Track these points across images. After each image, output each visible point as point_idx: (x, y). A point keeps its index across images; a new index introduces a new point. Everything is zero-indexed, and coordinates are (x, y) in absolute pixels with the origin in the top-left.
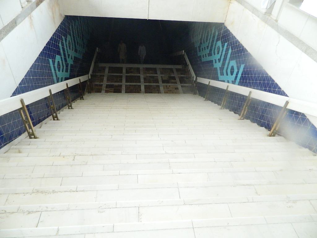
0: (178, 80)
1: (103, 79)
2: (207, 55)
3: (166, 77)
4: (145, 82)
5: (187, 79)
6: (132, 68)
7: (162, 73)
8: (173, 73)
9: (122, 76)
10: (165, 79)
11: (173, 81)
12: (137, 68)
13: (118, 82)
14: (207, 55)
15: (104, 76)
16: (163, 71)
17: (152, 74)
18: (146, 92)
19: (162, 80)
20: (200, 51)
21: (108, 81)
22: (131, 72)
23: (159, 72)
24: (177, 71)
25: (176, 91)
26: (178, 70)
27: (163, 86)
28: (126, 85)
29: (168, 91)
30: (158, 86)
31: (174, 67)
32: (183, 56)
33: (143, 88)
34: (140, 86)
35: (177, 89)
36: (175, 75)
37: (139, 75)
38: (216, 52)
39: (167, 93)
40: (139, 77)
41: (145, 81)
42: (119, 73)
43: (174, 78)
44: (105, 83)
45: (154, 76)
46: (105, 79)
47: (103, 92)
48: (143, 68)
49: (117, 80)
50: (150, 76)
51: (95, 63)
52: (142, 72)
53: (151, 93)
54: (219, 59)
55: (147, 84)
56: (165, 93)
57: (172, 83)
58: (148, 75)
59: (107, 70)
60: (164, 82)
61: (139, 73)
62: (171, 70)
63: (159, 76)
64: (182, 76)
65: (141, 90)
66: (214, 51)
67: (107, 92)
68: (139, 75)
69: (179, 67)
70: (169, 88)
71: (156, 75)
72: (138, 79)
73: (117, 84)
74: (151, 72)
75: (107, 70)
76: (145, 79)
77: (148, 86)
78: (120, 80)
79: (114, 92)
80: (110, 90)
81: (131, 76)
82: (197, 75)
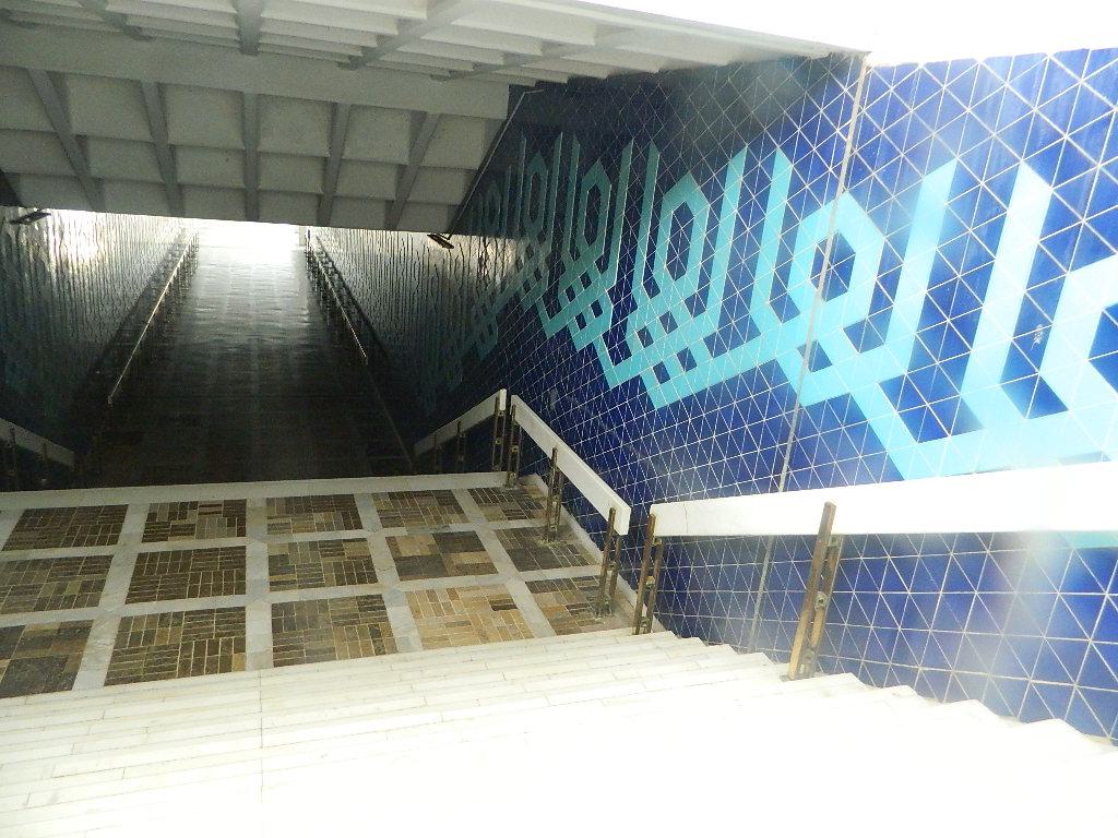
0: (496, 550)
2: (700, 352)
3: (417, 540)
4: (275, 585)
5: (553, 536)
6: (194, 505)
7: (388, 520)
8: (460, 511)
9: (109, 558)
10: (418, 552)
11: (467, 558)
12: (227, 503)
13: (70, 603)
14: (700, 352)
16: (397, 509)
20: (621, 353)
22: (188, 531)
23: (369, 515)
24: (478, 501)
25: (499, 619)
26: (483, 497)
27: (409, 594)
28: (125, 622)
29: (449, 625)
30: (374, 605)
31: (458, 483)
33: (258, 629)
34: (236, 618)
35: (504, 605)
37: (236, 542)
38: (801, 286)
39: (443, 641)
40: (237, 558)
41: (276, 578)
42: (91, 543)
43: (472, 542)
45: (339, 543)
48: (270, 502)
49: (61, 589)
50: (313, 545)
52: (256, 524)
56: (429, 642)
57: (464, 570)
58: (299, 538)
60: (408, 568)
61: (242, 533)
62: (446, 500)
63: (373, 535)
64: (516, 524)
65: (241, 647)
68: (236, 542)
69: (492, 480)
70: (449, 610)
72: (230, 570)
73: (51, 619)
74: (319, 517)
76: (278, 564)
77: (300, 605)
78: (85, 587)
81: (176, 554)
82: (640, 495)
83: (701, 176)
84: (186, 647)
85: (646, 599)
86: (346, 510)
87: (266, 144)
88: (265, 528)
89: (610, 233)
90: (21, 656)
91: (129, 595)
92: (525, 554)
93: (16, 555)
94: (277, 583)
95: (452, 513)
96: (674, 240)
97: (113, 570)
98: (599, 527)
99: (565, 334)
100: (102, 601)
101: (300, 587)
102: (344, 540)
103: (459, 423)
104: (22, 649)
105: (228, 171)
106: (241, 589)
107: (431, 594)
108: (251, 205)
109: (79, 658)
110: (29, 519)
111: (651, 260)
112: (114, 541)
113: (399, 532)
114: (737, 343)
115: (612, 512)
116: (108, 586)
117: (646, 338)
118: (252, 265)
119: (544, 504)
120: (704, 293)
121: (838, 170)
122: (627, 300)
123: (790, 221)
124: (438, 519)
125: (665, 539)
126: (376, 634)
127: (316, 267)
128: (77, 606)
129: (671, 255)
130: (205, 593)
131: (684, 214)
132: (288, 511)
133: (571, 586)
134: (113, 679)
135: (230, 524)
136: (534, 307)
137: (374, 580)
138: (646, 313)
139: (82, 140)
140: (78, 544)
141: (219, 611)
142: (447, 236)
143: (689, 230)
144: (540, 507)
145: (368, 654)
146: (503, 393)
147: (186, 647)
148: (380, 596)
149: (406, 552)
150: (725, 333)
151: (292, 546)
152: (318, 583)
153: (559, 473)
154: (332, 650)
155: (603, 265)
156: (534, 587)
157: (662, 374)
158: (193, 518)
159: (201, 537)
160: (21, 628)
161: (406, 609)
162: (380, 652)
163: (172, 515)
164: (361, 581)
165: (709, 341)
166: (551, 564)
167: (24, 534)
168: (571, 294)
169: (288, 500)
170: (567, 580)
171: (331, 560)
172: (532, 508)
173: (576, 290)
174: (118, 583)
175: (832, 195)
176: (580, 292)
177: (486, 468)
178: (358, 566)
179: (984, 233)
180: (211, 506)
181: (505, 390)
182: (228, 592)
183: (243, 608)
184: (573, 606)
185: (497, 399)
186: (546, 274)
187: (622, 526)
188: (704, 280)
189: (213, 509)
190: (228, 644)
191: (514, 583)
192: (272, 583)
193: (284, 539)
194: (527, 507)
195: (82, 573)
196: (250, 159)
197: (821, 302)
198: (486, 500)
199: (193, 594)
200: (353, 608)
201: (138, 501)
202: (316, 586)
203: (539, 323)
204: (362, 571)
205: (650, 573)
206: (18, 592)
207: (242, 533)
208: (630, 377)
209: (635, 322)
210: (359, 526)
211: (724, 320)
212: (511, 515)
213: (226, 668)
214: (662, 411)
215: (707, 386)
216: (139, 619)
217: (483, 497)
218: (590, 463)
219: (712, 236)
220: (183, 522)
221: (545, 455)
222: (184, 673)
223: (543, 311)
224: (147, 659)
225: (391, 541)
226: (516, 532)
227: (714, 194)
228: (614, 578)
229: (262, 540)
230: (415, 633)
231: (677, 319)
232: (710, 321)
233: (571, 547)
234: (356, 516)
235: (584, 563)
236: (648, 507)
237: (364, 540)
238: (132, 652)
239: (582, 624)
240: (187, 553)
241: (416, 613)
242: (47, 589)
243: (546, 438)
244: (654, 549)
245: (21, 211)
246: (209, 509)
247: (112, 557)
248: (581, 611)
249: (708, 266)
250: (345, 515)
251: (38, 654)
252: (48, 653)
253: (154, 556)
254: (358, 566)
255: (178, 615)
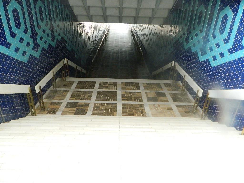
0: (169, 97)
1: (66, 95)
2: (226, 53)
3: (152, 94)
6: (108, 83)
7: (146, 89)
8: (162, 88)
11: (163, 98)
13: (86, 99)
14: (226, 53)
15: (68, 91)
16: (148, 87)
17: (134, 89)
18: (124, 114)
19: (147, 97)
21: (72, 98)
22: (106, 88)
23: (142, 87)
24: (166, 86)
25: (169, 112)
26: (167, 85)
28: (95, 104)
30: (141, 106)
31: (162, 82)
32: (173, 69)
33: (119, 108)
34: (115, 106)
35: (170, 109)
36: (165, 91)
37: (115, 90)
39: (156, 115)
43: (163, 95)
44: (67, 99)
45: (135, 93)
46: (69, 95)
47: (59, 113)
49: (84, 97)
50: (130, 92)
51: (57, 75)
52: (119, 87)
53: (132, 115)
55: (126, 102)
56: (153, 115)
57: (162, 101)
58: (127, 91)
59: (75, 85)
60: (150, 99)
61: (116, 89)
62: (159, 85)
63: (143, 92)
64: (174, 92)
65: (116, 111)
67: (64, 113)
68: (115, 90)
70: (158, 109)
71: (138, 91)
72: (114, 96)
74: (132, 87)
75: (75, 85)
76: (123, 96)
77: (127, 104)
78: (88, 97)
79: (76, 113)
80: (70, 110)
82: (205, 88)
83: (232, 6)
84: (106, 110)
85: (205, 112)
86: (137, 86)
87: (124, 6)
88: (121, 88)
89: (204, 23)
90: (77, 108)
91: (96, 99)
92: (175, 99)
93: (77, 89)
94: (123, 99)
95: (160, 88)
96: (222, 24)
97: (93, 94)
98: (194, 94)
99: (190, 48)
100: (91, 99)
101: (127, 101)
102: (137, 92)
103: (163, 68)
104: (78, 107)
105: (116, 12)
106: (116, 100)
107: (154, 105)
108: (120, 20)
109: (88, 109)
110: (79, 83)
111: (215, 30)
112: (93, 88)
113: (148, 91)
114: (237, 50)
115: (198, 91)
116: (92, 97)
117: (211, 49)
118: (120, 33)
119: (181, 88)
120: (229, 38)
122: (207, 40)
124: (157, 90)
125: (211, 98)
126: (142, 112)
128: (87, 100)
129: (221, 28)
130: (109, 100)
131: (226, 17)
132: (126, 85)
133: (186, 107)
134: (93, 114)
135: (114, 87)
136: (183, 42)
137: (142, 101)
138: (213, 43)
139: (89, 7)
140: (87, 88)
141: (112, 104)
142: (163, 25)
143: (226, 21)
144: (180, 88)
145: (140, 116)
146: (173, 62)
147: (106, 110)
148: (143, 104)
149: (149, 96)
150: (234, 48)
151: (126, 92)
152: (131, 100)
153: (185, 81)
154: (133, 114)
155: (201, 31)
156: (177, 106)
157: (215, 58)
158: (107, 85)
159: (109, 89)
160: (78, 103)
161: (149, 108)
162: (143, 116)
163: (104, 84)
164: (140, 101)
165: (229, 50)
166: (181, 101)
167: (79, 86)
168: (192, 38)
169: (126, 83)
170: (185, 106)
171: (134, 96)
172: (178, 88)
173: (194, 37)
174: (94, 96)
176: (195, 38)
177: (168, 79)
178: (139, 98)
180: (111, 83)
181: (174, 61)
182: (114, 100)
183: (116, 104)
184: (187, 111)
185: (172, 63)
186: (186, 33)
187: (200, 94)
188: (229, 34)
189: (112, 84)
190: (113, 110)
191: (173, 105)
192: (122, 99)
193: (125, 91)
194: (177, 88)
195: (88, 94)
196: (121, 9)
198: (167, 86)
199: (107, 100)
200: (138, 106)
201: (98, 81)
202: (130, 101)
203: (183, 46)
204: (139, 99)
205: (206, 106)
206: (77, 96)
207: (116, 89)
208: (206, 59)
209: (209, 45)
210: (140, 89)
211: (234, 44)
212: (173, 90)
213: (113, 115)
214: (214, 67)
215: (227, 62)
216: (98, 104)
217: (167, 85)
218: (194, 80)
219: (233, 23)
220: (106, 86)
221: (182, 77)
222: (105, 115)
223: (185, 43)
224: (99, 111)
225: (146, 93)
226: (174, 94)
227: (235, 11)
228: (197, 106)
229: (120, 91)
230: (150, 113)
231: (220, 45)
232: (230, 45)
233: (187, 98)
234: (139, 87)
235: (190, 102)
236: (207, 90)
237: (141, 92)
238: (97, 109)
239: (188, 115)
240: (106, 92)
241: (151, 109)
242: (82, 96)
243: (183, 73)
244: (208, 101)
245: (78, 23)
246: (110, 83)
247: (93, 91)
248: (188, 112)
249: (231, 30)
250: (137, 87)
251: (81, 108)
252: (82, 108)
253: (100, 92)
254: (139, 98)
255: (104, 104)
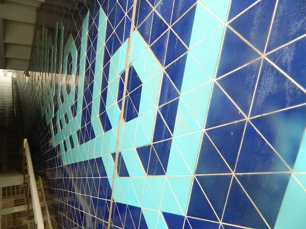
54: (143, 152)
66: (103, 107)
120: (76, 103)
121: (130, 14)
123: (107, 59)
127: (15, 83)
150: (83, 129)
175: (128, 35)
179: (288, 58)
181: (26, 139)
197: (122, 121)
